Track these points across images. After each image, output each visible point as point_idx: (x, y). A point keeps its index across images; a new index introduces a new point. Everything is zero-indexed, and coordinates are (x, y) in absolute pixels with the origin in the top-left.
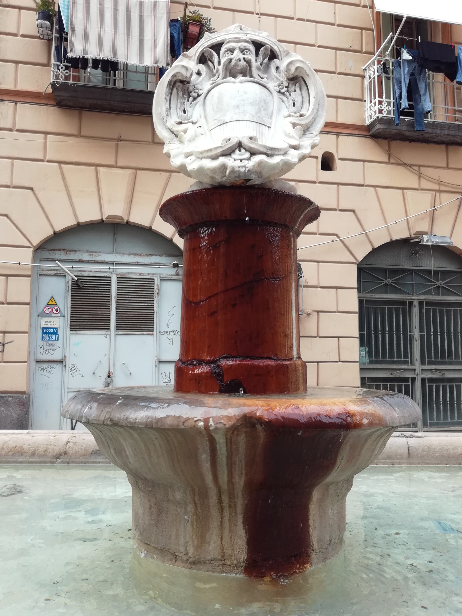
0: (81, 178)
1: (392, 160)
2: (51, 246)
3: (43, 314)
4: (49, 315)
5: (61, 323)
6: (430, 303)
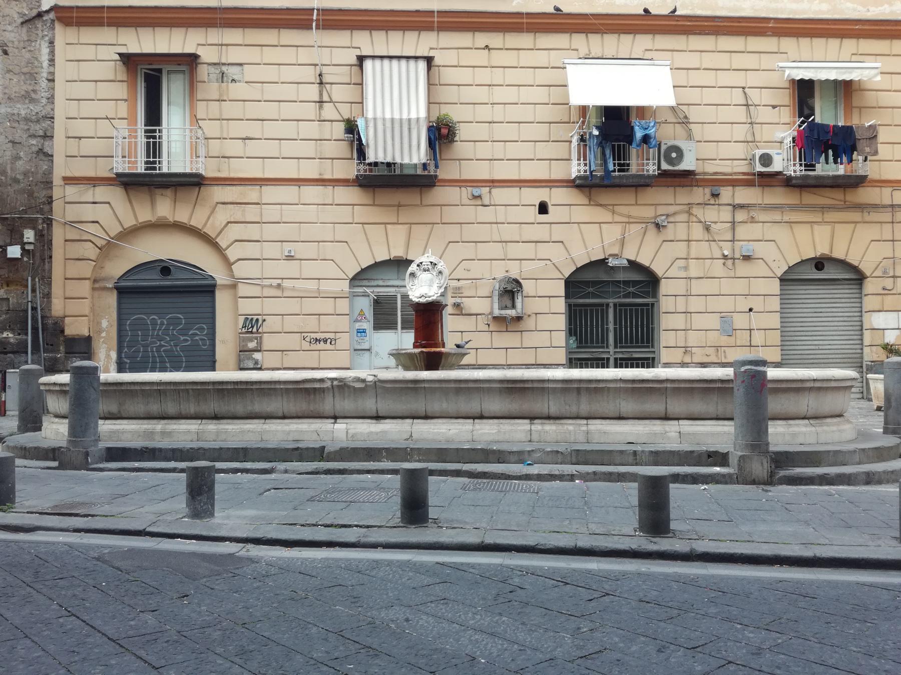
0: (376, 232)
1: (592, 202)
2: (359, 278)
3: (356, 321)
4: (360, 321)
5: (367, 325)
6: (621, 305)
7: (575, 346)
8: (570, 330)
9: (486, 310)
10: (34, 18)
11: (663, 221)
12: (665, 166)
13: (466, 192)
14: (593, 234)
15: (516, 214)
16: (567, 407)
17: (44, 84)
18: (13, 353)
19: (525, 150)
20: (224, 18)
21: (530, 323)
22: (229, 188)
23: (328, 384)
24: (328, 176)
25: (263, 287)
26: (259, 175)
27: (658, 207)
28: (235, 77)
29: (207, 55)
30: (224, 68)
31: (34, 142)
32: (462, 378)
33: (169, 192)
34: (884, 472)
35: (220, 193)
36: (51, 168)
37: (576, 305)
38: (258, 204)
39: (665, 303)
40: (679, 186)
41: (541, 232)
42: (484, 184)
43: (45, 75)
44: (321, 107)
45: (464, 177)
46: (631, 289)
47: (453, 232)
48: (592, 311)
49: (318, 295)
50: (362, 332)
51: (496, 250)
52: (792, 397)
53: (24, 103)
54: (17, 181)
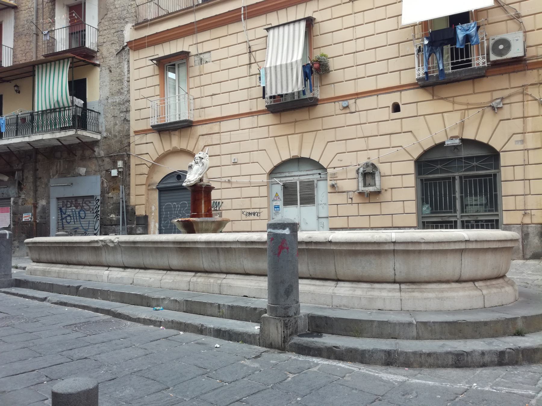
0: (282, 141)
1: (435, 97)
2: (275, 171)
3: (274, 200)
4: (276, 200)
5: (280, 203)
6: (466, 177)
7: (428, 211)
8: (423, 199)
9: (354, 188)
10: (121, 50)
11: (499, 103)
12: (493, 58)
13: (339, 105)
14: (437, 122)
15: (374, 116)
16: (213, 264)
17: (126, 83)
18: (115, 225)
19: (380, 67)
20: (200, 27)
21: (386, 196)
22: (204, 126)
23: (100, 244)
24: (254, 110)
25: (221, 182)
26: (219, 116)
27: (494, 93)
28: (207, 60)
29: (193, 51)
30: (202, 56)
31: (122, 115)
32: (74, 241)
33: (177, 133)
34: (415, 353)
35: (201, 129)
36: (129, 127)
37: (426, 180)
38: (219, 133)
39: (505, 173)
40: (514, 72)
41: (394, 126)
42: (351, 98)
43: (126, 79)
44: (250, 67)
45: (338, 94)
46: (475, 164)
47: (330, 135)
48: (440, 184)
49: (250, 185)
50: (277, 207)
51: (360, 144)
52: (373, 259)
53: (118, 96)
54: (115, 136)
